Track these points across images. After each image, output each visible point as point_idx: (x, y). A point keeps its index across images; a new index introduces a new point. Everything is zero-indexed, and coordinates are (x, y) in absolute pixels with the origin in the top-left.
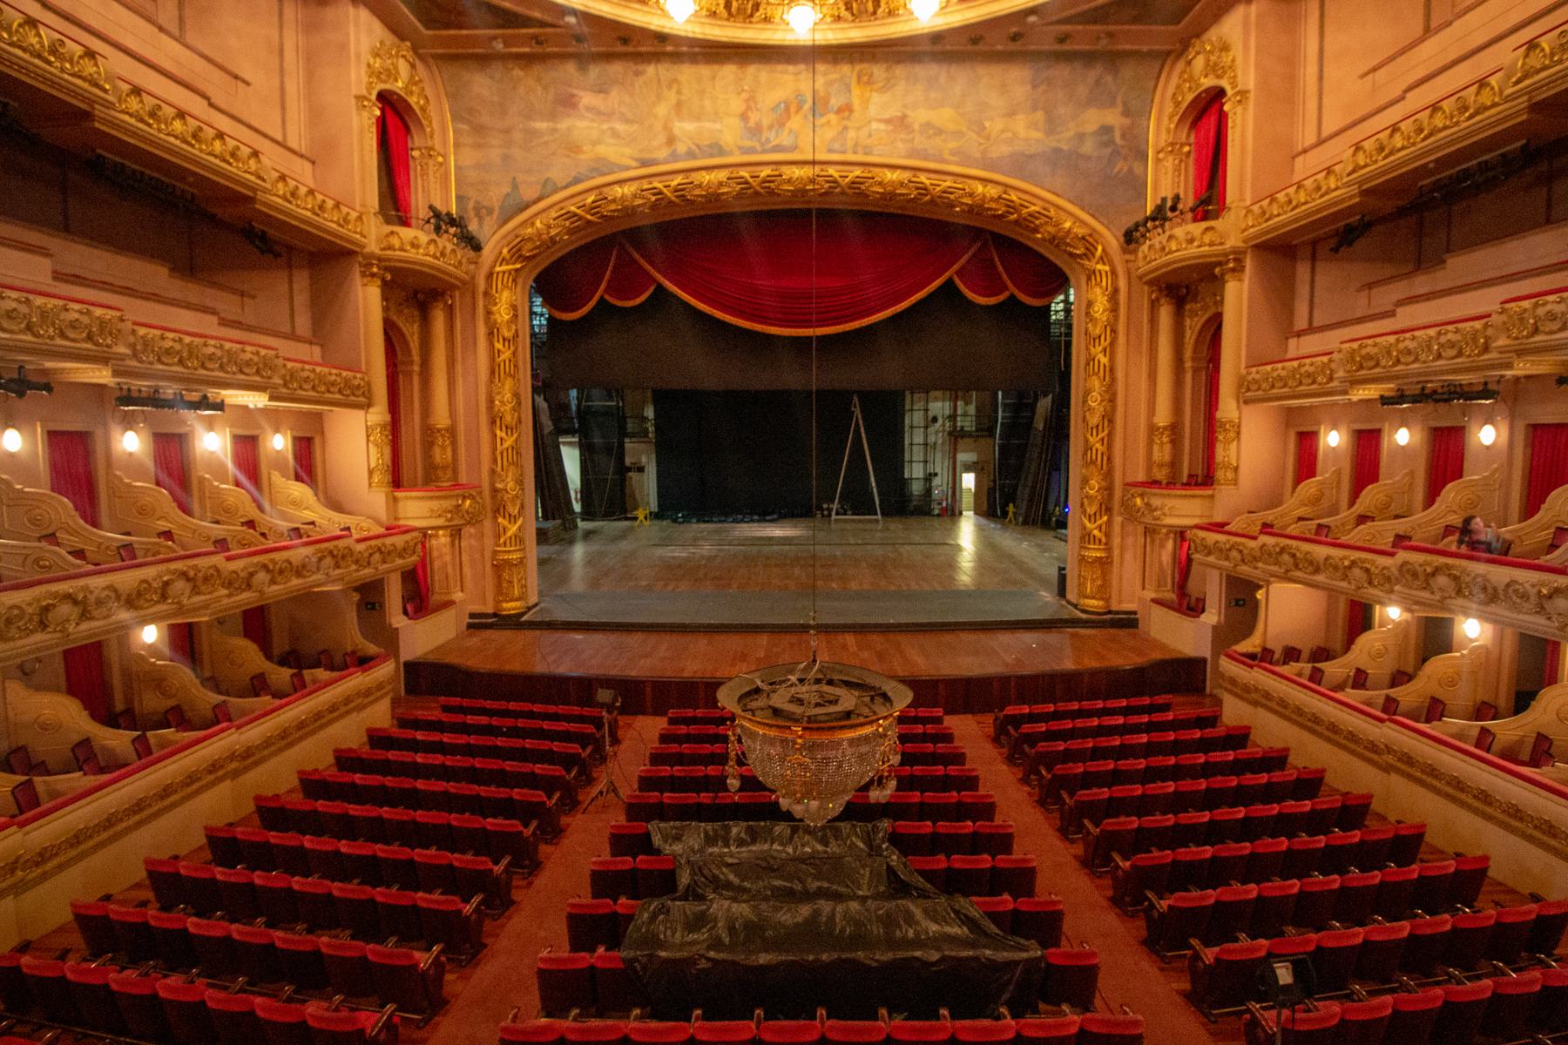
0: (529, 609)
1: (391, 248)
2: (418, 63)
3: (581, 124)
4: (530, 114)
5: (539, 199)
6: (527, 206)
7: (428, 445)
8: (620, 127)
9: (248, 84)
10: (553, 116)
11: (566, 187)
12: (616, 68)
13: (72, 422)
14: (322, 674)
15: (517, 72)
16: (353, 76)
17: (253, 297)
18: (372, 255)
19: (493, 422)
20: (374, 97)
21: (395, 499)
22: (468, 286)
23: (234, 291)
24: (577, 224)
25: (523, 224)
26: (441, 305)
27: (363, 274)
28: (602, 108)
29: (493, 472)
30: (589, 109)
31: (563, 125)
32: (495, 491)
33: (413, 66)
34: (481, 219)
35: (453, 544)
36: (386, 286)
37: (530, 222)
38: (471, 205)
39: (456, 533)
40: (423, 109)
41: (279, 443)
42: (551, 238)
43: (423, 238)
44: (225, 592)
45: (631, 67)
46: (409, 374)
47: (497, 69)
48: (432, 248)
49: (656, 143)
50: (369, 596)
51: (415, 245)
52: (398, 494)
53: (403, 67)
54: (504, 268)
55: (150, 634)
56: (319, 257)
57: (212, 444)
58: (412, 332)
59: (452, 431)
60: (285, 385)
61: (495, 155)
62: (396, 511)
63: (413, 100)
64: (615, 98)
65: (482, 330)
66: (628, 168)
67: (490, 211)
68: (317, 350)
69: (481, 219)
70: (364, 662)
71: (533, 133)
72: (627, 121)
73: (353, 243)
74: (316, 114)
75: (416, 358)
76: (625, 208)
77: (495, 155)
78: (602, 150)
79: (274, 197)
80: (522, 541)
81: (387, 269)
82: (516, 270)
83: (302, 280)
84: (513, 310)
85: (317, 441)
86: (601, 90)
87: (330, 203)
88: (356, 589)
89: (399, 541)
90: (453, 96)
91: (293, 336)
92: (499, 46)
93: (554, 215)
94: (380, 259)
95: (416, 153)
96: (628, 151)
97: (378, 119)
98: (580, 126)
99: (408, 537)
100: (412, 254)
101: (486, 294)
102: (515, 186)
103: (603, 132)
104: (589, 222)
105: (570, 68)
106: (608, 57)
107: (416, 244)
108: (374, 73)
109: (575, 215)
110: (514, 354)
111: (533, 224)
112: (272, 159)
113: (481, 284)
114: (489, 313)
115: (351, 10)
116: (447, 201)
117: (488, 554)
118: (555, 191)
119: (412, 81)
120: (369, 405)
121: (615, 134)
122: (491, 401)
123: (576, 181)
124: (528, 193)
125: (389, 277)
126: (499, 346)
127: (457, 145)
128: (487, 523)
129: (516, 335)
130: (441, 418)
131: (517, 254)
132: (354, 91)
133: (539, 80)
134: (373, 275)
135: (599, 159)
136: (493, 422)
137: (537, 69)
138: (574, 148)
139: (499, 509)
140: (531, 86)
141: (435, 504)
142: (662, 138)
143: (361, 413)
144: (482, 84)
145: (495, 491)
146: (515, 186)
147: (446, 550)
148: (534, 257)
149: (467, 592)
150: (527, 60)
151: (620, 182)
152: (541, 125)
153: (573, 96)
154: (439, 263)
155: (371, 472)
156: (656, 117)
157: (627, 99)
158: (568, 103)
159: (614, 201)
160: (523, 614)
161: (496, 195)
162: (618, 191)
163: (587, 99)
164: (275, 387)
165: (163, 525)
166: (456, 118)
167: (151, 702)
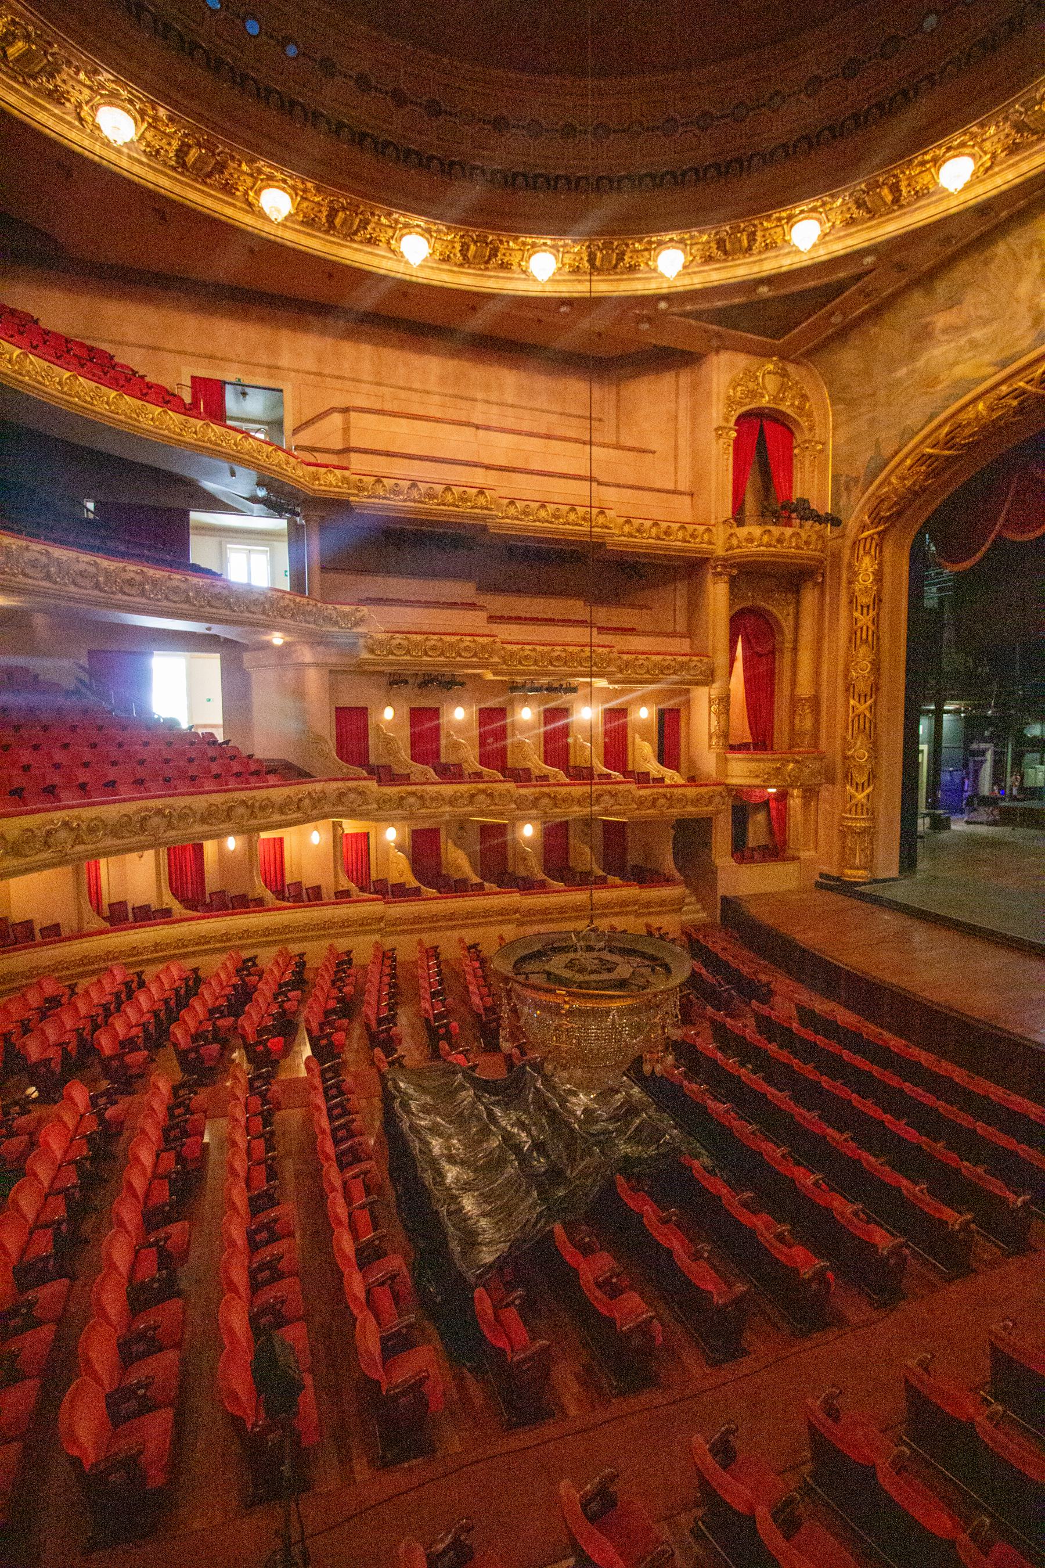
0: (876, 881)
1: (731, 548)
2: (791, 368)
3: (936, 352)
4: (892, 364)
5: (897, 453)
6: (886, 465)
7: (793, 713)
8: (978, 334)
9: (654, 452)
10: (912, 357)
11: (922, 428)
12: (962, 271)
13: (492, 703)
14: (617, 880)
15: (874, 330)
16: (714, 411)
17: (647, 607)
18: (717, 559)
19: (848, 690)
20: (732, 424)
21: (726, 759)
22: (836, 557)
23: (633, 606)
24: (936, 467)
25: (881, 485)
26: (810, 584)
27: (715, 574)
28: (959, 322)
29: (844, 739)
30: (944, 331)
31: (920, 363)
32: (846, 758)
33: (784, 374)
34: (847, 488)
35: (806, 806)
36: (733, 582)
37: (886, 481)
38: (843, 480)
39: (810, 793)
40: (801, 408)
41: (644, 714)
42: (909, 489)
43: (757, 531)
44: (513, 806)
45: (977, 258)
46: (781, 651)
47: (856, 339)
48: (766, 538)
49: (1017, 333)
50: (691, 835)
51: (750, 540)
52: (729, 756)
53: (771, 384)
54: (866, 534)
55: (528, 830)
56: (690, 569)
57: (586, 715)
58: (783, 614)
59: (815, 701)
60: (621, 671)
61: (862, 424)
62: (726, 768)
63: (785, 407)
64: (974, 304)
65: (844, 600)
66: (984, 379)
67: (856, 480)
68: (686, 642)
69: (847, 488)
70: (668, 881)
71: (892, 386)
72: (986, 322)
73: (705, 552)
74: (696, 454)
75: (789, 636)
76: (984, 428)
77: (862, 424)
78: (960, 371)
79: (619, 537)
80: (872, 813)
81: (731, 566)
82: (879, 533)
83: (682, 588)
84: (873, 574)
85: (683, 714)
86: (953, 303)
87: (675, 526)
88: (673, 827)
89: (691, 792)
90: (830, 384)
91: (674, 635)
92: (837, 319)
93: (908, 462)
94: (726, 560)
95: (796, 451)
96: (987, 358)
97: (736, 441)
98: (938, 353)
99: (702, 790)
100: (753, 548)
101: (850, 566)
102: (877, 445)
103: (961, 349)
104: (948, 457)
105: (918, 297)
106: (947, 264)
107: (756, 538)
108: (730, 402)
109: (931, 456)
110: (876, 621)
111: (890, 483)
112: (652, 506)
113: (846, 557)
114: (850, 582)
115: (715, 359)
116: (822, 485)
117: (837, 817)
118: (911, 438)
119: (783, 388)
120: (713, 682)
121: (974, 344)
122: (847, 670)
123: (932, 417)
124: (887, 452)
125: (735, 572)
126: (856, 614)
127: (835, 428)
128: (838, 787)
129: (878, 600)
130: (804, 690)
131: (876, 517)
132: (715, 426)
133: (892, 328)
134: (721, 574)
135: (956, 382)
136: (848, 690)
137: (888, 317)
138: (930, 381)
139: (847, 776)
140: (888, 336)
141: (753, 766)
142: (1027, 323)
143: (706, 689)
144: (848, 359)
145: (846, 758)
146: (877, 445)
147: (798, 810)
148: (899, 514)
149: (815, 852)
150: (876, 313)
151: (974, 401)
152: (902, 372)
153: (926, 326)
154: (779, 549)
155: (710, 737)
156: (1017, 301)
157: (983, 298)
158: (924, 335)
159: (969, 424)
160: (857, 884)
161: (863, 459)
162: (970, 414)
163: (941, 320)
164: (611, 673)
165: (529, 765)
166: (835, 400)
167: (522, 872)
